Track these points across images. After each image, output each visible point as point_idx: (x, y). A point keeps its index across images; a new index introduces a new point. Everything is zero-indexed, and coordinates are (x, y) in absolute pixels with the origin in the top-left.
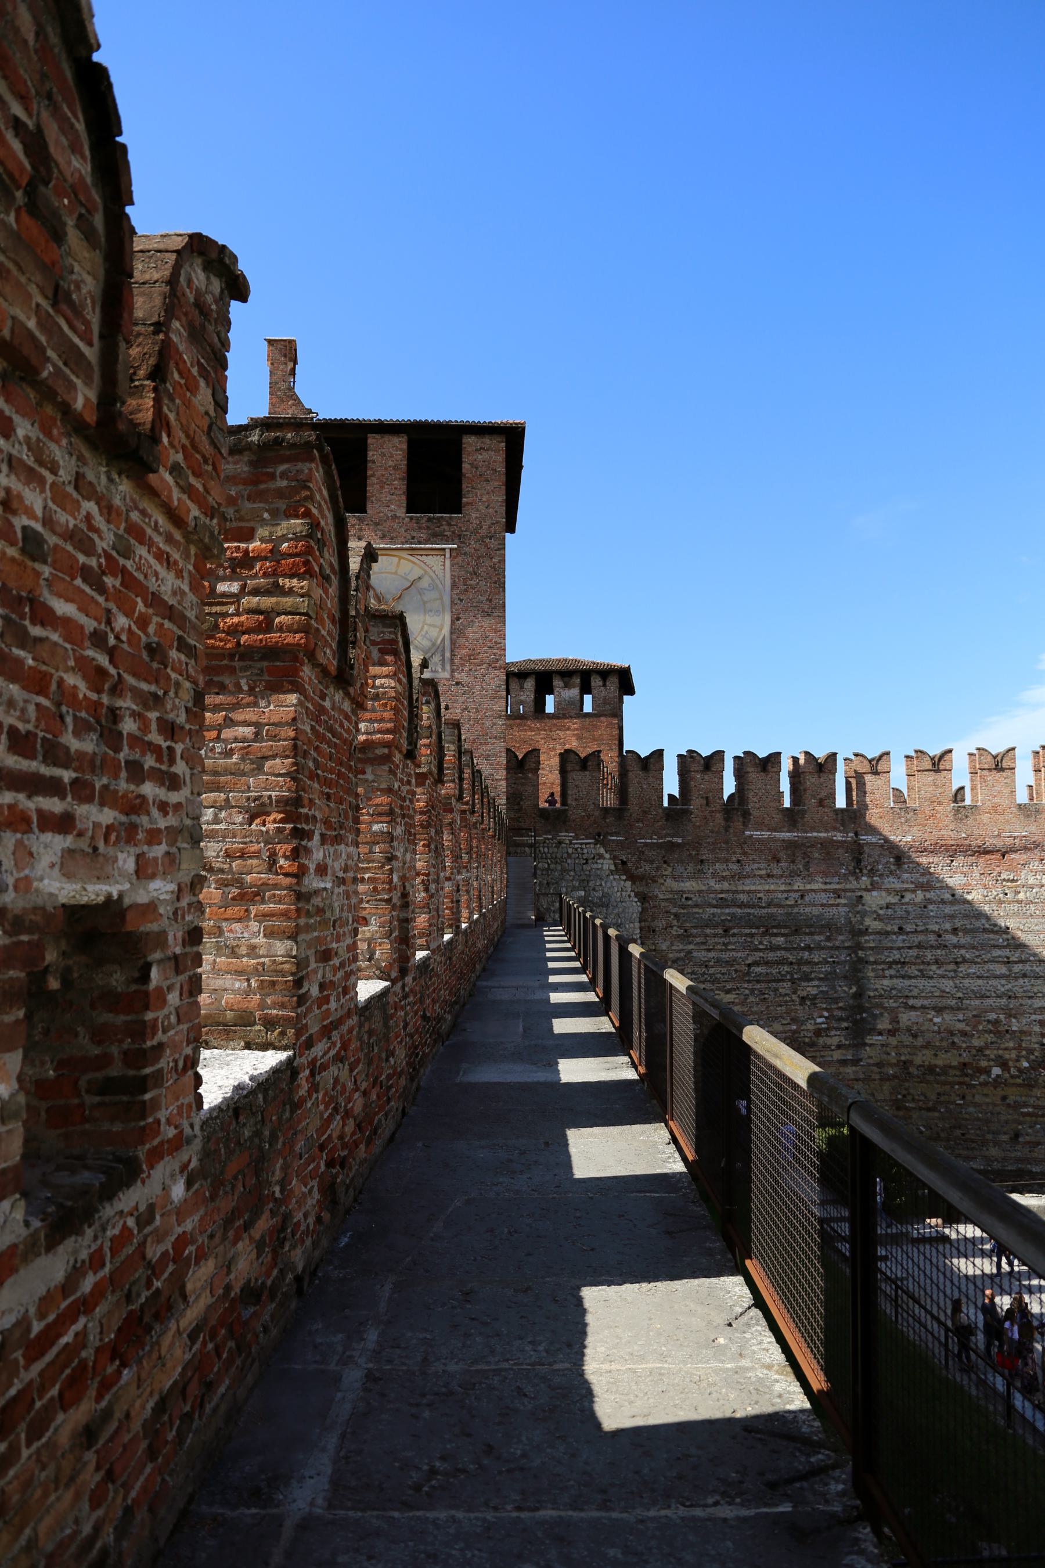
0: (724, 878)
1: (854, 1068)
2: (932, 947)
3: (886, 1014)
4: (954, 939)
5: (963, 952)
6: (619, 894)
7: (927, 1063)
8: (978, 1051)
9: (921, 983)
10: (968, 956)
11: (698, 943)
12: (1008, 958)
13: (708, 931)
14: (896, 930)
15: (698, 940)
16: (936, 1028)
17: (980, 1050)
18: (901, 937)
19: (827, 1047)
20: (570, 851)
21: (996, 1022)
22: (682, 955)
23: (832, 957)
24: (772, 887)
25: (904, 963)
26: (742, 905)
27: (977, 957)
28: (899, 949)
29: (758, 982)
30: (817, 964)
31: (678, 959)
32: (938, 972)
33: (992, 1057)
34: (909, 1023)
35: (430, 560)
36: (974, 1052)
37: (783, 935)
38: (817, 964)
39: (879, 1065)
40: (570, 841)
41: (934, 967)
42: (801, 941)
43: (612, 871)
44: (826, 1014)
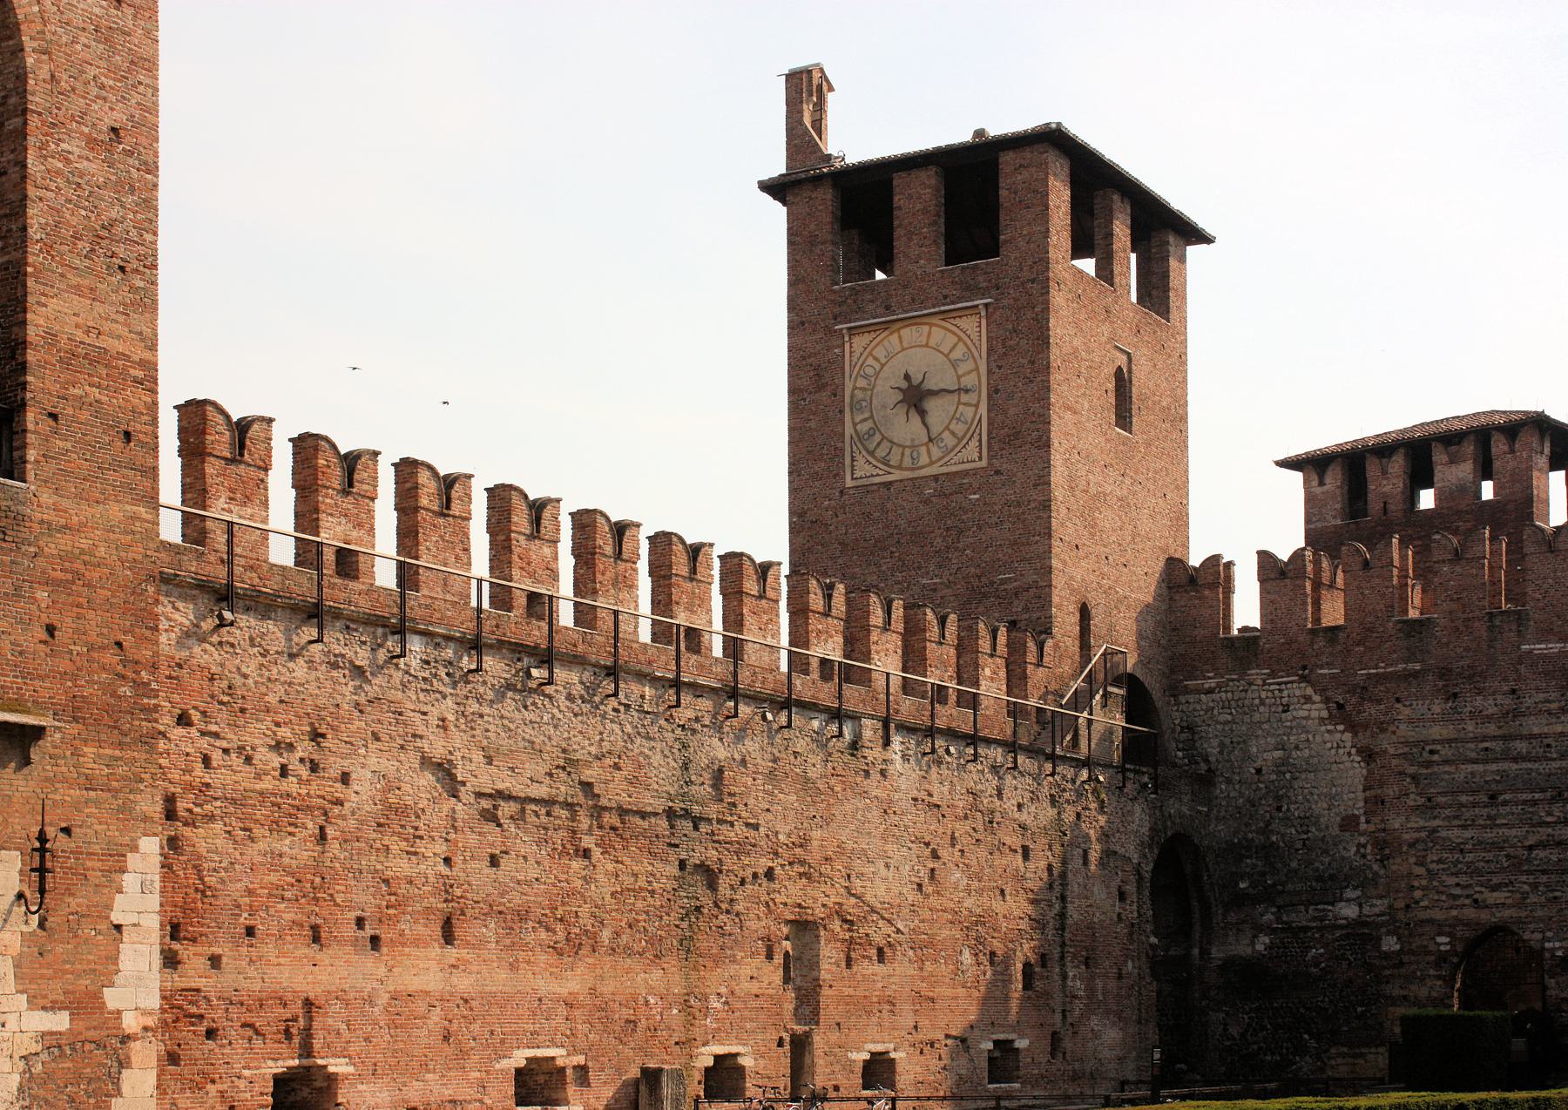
11: (1448, 817)
13: (1463, 799)
15: (1447, 812)
20: (1263, 695)
22: (1423, 834)
29: (1544, 872)
31: (1417, 841)
35: (962, 323)
40: (1264, 681)
43: (1322, 719)
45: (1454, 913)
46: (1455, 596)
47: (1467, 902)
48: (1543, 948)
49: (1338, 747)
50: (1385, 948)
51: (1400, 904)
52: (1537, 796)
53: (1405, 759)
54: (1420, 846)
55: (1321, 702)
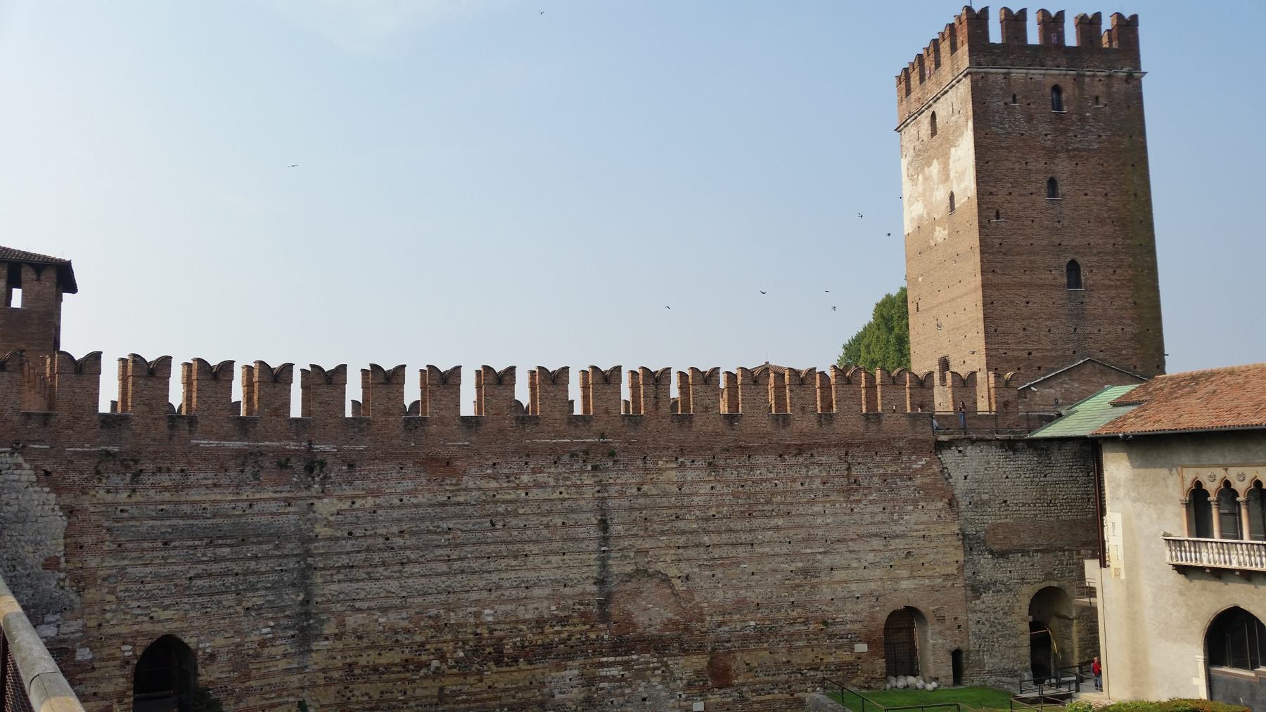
0: (166, 489)
1: (299, 676)
2: (379, 549)
3: (333, 619)
4: (400, 541)
5: (408, 553)
6: (40, 508)
7: (371, 663)
8: (419, 646)
9: (368, 585)
10: (413, 557)
11: (133, 558)
12: (449, 556)
13: (146, 545)
14: (346, 535)
15: (133, 554)
16: (381, 628)
17: (422, 645)
18: (350, 542)
19: (272, 658)
21: (437, 616)
22: (114, 571)
23: (280, 565)
24: (219, 497)
25: (352, 567)
26: (185, 516)
27: (421, 557)
28: (348, 553)
29: (200, 595)
30: (264, 573)
31: (109, 576)
32: (385, 573)
33: (433, 650)
34: (355, 626)
36: (416, 647)
37: (228, 546)
38: (264, 573)
39: (324, 670)
41: (381, 569)
42: (248, 551)
43: (31, 483)
44: (272, 624)
45: (136, 627)
46: (147, 402)
47: (146, 619)
48: (198, 649)
49: (44, 504)
50: (79, 658)
51: (93, 623)
52: (197, 543)
53: (103, 515)
54: (112, 580)
55: (31, 469)
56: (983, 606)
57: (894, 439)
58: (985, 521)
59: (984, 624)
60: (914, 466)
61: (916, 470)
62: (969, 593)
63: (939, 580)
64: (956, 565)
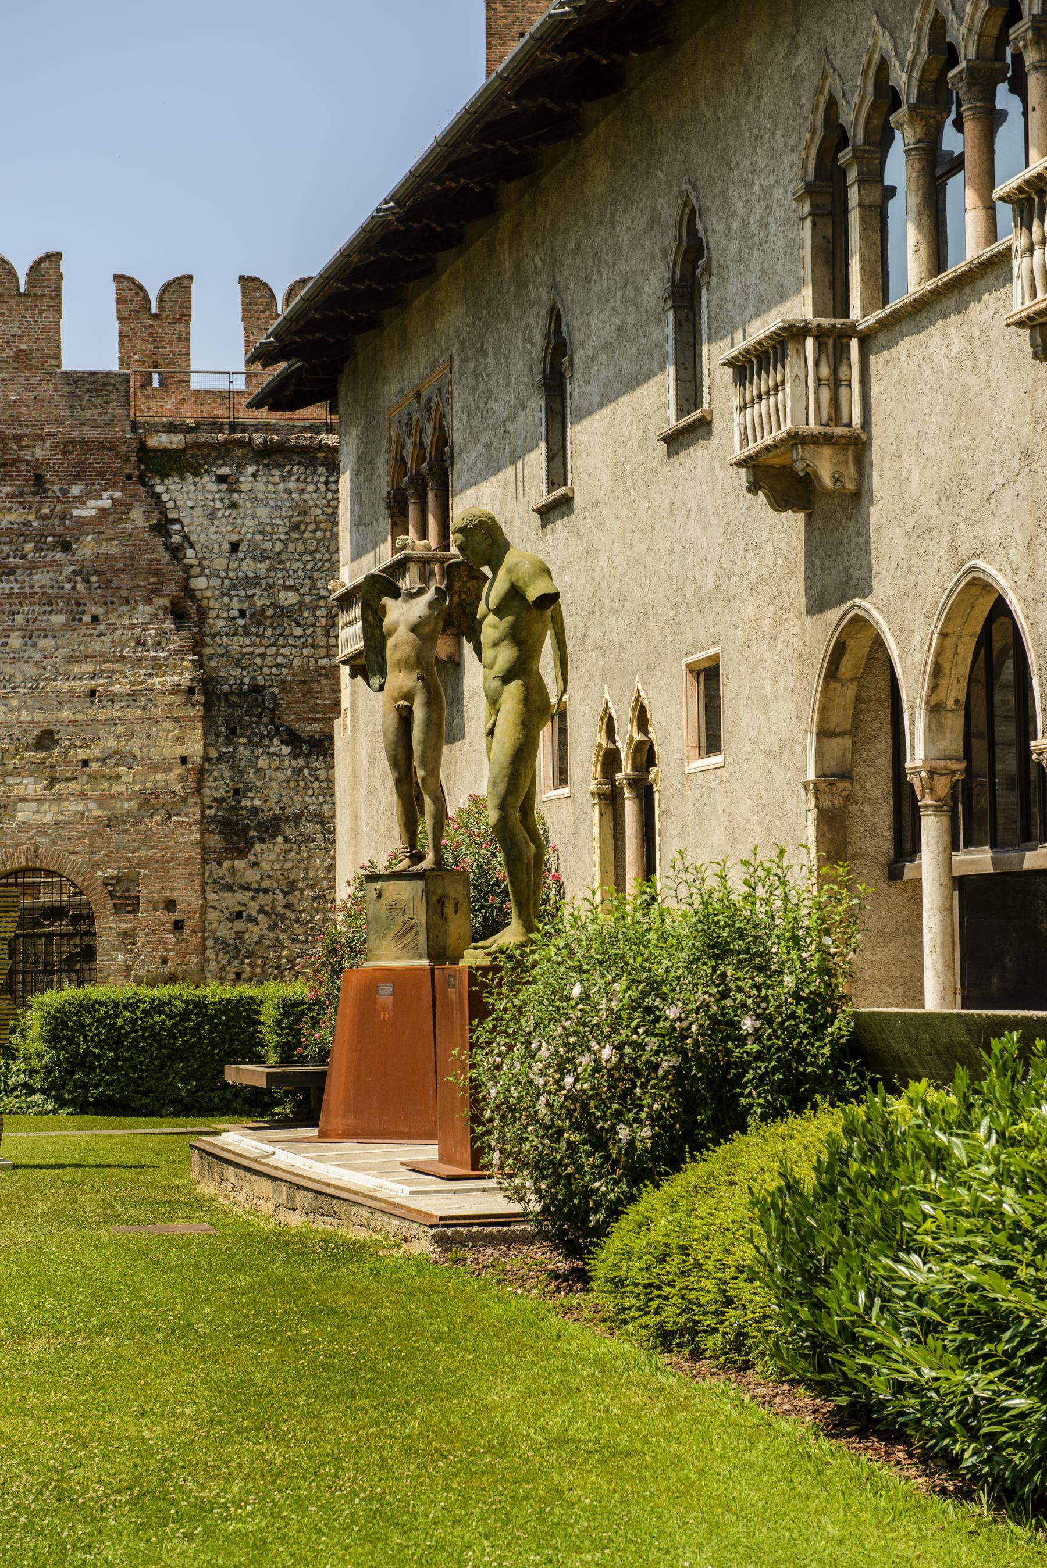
56: (252, 876)
57: (18, 438)
58: (280, 660)
59: (252, 920)
60: (76, 512)
61: (84, 523)
62: (215, 841)
63: (126, 805)
64: (179, 770)
